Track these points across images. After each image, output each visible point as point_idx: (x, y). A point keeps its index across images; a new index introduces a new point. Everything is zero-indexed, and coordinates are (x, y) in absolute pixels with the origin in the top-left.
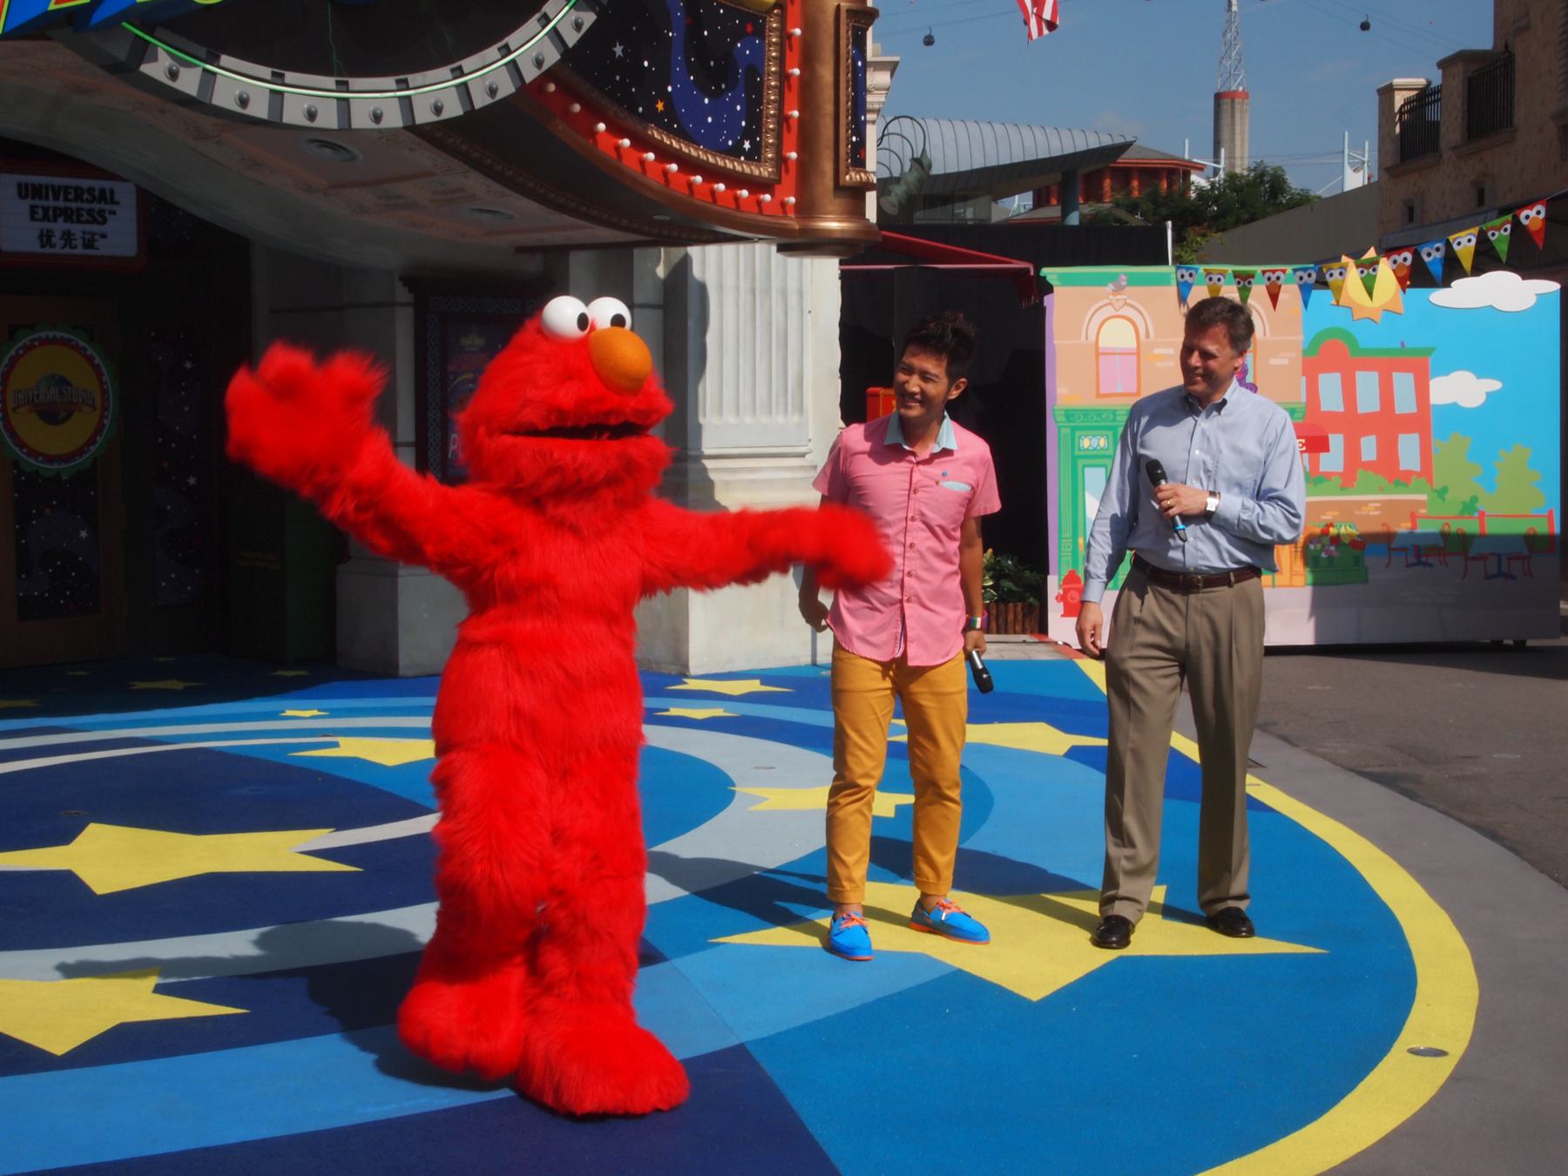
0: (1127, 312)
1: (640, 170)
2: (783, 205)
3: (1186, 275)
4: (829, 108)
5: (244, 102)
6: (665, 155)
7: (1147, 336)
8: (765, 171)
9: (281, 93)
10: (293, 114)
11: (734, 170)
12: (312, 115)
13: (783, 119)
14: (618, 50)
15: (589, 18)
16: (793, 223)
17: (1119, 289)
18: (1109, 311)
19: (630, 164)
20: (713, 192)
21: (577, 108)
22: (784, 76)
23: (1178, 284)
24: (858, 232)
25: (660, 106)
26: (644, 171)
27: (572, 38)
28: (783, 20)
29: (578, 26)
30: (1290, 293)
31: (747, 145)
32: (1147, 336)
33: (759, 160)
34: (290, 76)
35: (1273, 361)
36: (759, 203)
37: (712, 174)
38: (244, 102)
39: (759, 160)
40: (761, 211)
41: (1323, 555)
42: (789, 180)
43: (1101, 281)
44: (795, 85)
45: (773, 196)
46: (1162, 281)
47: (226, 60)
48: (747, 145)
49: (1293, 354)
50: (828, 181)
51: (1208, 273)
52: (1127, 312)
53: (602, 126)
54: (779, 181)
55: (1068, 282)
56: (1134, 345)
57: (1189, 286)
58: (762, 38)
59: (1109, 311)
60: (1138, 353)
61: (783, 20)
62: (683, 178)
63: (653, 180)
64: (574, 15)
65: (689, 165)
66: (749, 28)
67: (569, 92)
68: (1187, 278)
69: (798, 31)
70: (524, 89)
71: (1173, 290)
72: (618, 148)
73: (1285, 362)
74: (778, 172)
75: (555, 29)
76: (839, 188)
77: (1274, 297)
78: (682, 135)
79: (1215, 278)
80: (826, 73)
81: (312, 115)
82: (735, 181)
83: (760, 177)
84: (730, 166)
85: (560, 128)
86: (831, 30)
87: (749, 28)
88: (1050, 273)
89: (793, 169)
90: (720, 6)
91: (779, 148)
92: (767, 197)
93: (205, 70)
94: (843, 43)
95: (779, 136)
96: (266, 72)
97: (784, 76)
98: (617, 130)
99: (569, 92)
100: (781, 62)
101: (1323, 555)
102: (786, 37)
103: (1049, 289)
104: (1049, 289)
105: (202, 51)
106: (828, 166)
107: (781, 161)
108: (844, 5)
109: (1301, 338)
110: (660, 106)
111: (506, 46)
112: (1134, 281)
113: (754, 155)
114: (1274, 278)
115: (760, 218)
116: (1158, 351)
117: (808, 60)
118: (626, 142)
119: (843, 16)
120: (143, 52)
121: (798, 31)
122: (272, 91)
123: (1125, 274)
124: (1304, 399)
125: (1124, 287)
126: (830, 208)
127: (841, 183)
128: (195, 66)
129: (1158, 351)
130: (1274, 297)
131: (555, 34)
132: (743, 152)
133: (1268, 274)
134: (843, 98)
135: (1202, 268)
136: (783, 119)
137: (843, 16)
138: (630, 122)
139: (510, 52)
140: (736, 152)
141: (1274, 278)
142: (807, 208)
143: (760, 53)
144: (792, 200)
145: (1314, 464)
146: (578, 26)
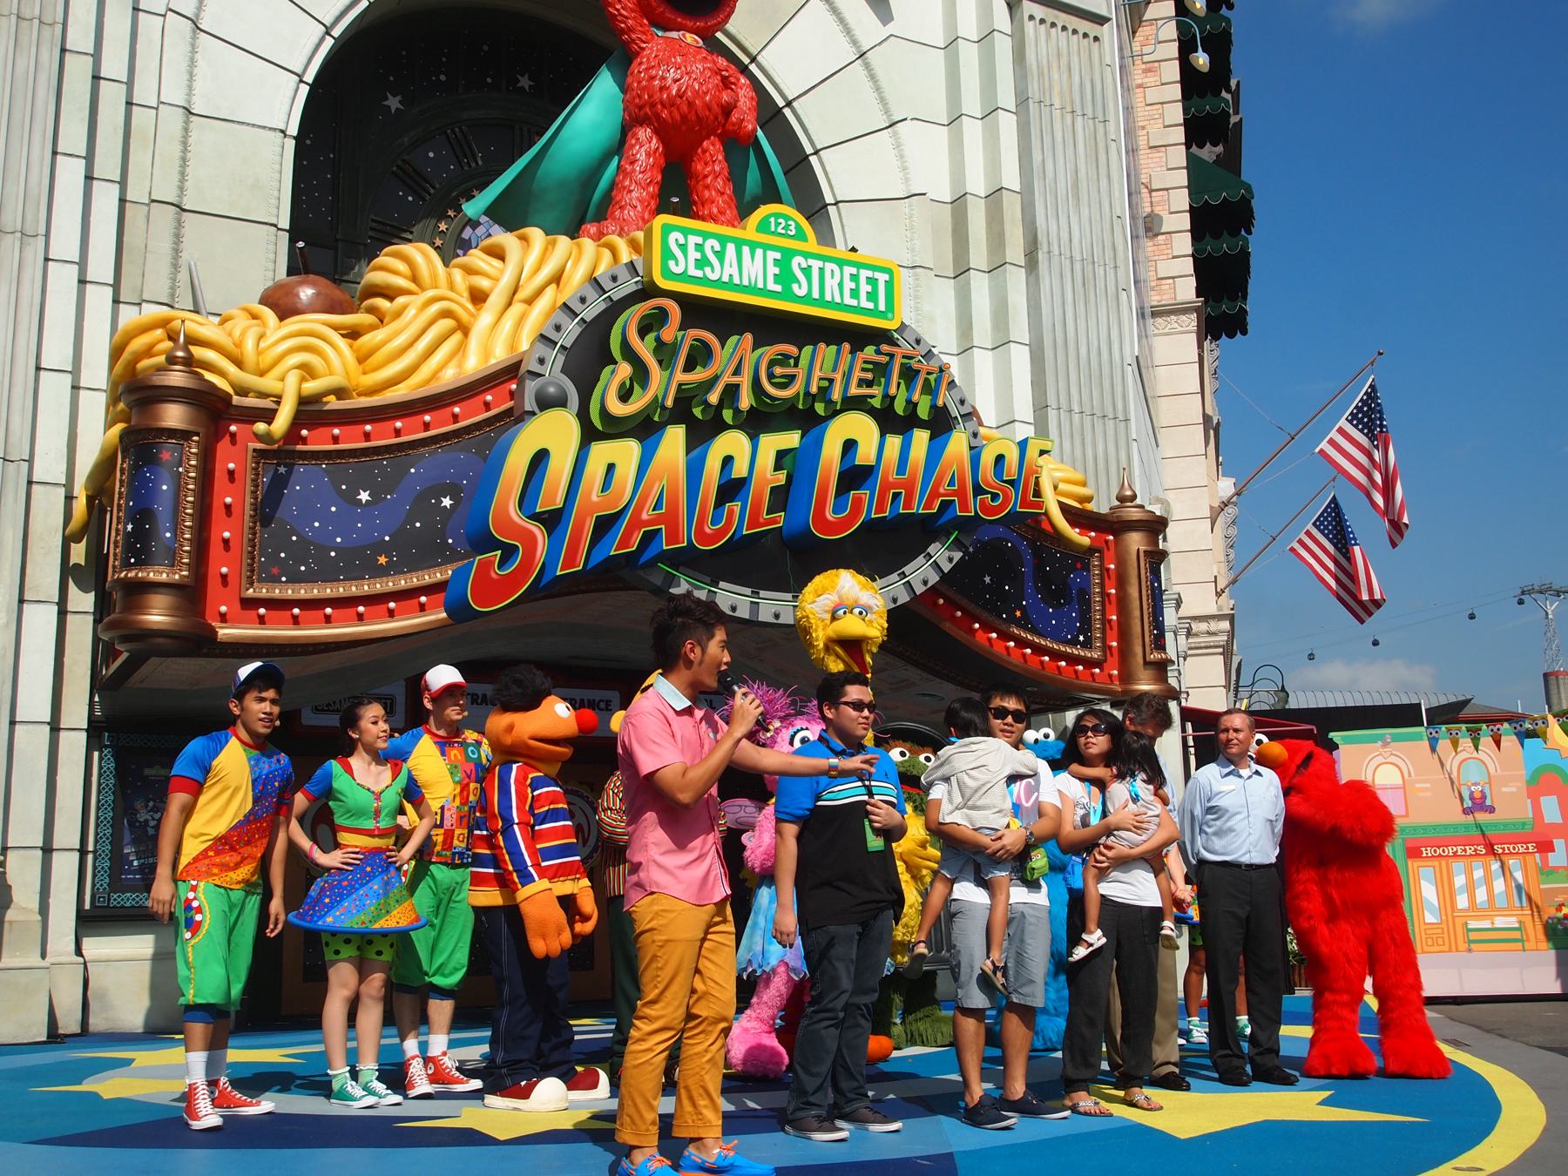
0: (1392, 759)
1: (988, 644)
2: (1110, 676)
3: (1434, 734)
4: (1137, 613)
5: (734, 609)
6: (1022, 643)
7: (1410, 776)
8: (1096, 655)
9: (758, 603)
10: (765, 615)
11: (1072, 653)
12: (777, 616)
13: (1105, 622)
14: (987, 579)
15: (957, 555)
16: (1117, 687)
17: (1385, 744)
18: (1380, 759)
19: (999, 648)
20: (1059, 668)
21: (959, 614)
22: (1104, 594)
23: (1429, 739)
24: (1161, 690)
25: (1018, 614)
26: (1009, 654)
27: (947, 567)
28: (1101, 559)
29: (951, 560)
30: (1509, 741)
31: (1081, 638)
32: (1410, 776)
33: (1091, 648)
34: (763, 593)
35: (1504, 789)
36: (1093, 675)
37: (1056, 656)
38: (734, 609)
39: (1091, 648)
40: (1094, 680)
41: (1559, 927)
42: (1113, 660)
43: (1373, 740)
44: (1113, 599)
45: (1102, 670)
46: (1418, 737)
47: (722, 584)
48: (1081, 638)
49: (1519, 784)
50: (1140, 661)
51: (1448, 730)
52: (1392, 759)
53: (977, 626)
54: (1105, 661)
55: (1348, 741)
56: (1400, 782)
57: (1437, 740)
58: (1088, 571)
59: (1380, 759)
60: (1404, 787)
61: (1101, 559)
62: (1036, 658)
63: (1015, 659)
64: (947, 554)
65: (1039, 650)
66: (1079, 566)
67: (952, 604)
68: (1434, 734)
69: (1112, 566)
70: (916, 598)
71: (1426, 743)
72: (990, 640)
73: (1514, 790)
74: (1104, 652)
75: (935, 561)
76: (1146, 663)
77: (1498, 743)
78: (1034, 631)
79: (1454, 732)
80: (1133, 591)
81: (777, 616)
82: (1073, 660)
83: (1092, 658)
84: (1069, 650)
85: (947, 626)
86: (1136, 565)
87: (1079, 566)
88: (1335, 736)
89: (1115, 652)
90: (1057, 552)
91: (1104, 640)
92: (1097, 670)
93: (709, 591)
94: (1143, 572)
95: (1104, 632)
96: (748, 591)
97: (1104, 594)
98: (987, 628)
99: (952, 604)
100: (1102, 585)
101: (1559, 927)
102: (1105, 571)
103: (1336, 747)
104: (1336, 747)
105: (708, 580)
106: (1138, 650)
107: (1106, 648)
108: (1142, 548)
109: (1524, 772)
110: (1018, 614)
111: (903, 572)
112: (1395, 739)
113: (1087, 644)
114: (1495, 729)
115: (1094, 684)
116: (1417, 786)
117: (1121, 584)
118: (994, 635)
119: (1142, 555)
120: (671, 580)
121: (1112, 566)
122: (751, 602)
123: (1390, 734)
124: (1531, 815)
125: (1389, 743)
126: (1142, 677)
127: (1148, 660)
128: (705, 588)
129: (1417, 786)
130: (1498, 743)
131: (936, 565)
132: (1079, 642)
133: (1491, 727)
134: (1145, 606)
135: (1444, 728)
136: (1105, 622)
137: (1142, 555)
138: (998, 623)
139: (906, 577)
140: (1074, 642)
141: (1495, 729)
142: (1126, 677)
143: (1087, 580)
144: (1115, 672)
145: (1545, 861)
146: (951, 560)
